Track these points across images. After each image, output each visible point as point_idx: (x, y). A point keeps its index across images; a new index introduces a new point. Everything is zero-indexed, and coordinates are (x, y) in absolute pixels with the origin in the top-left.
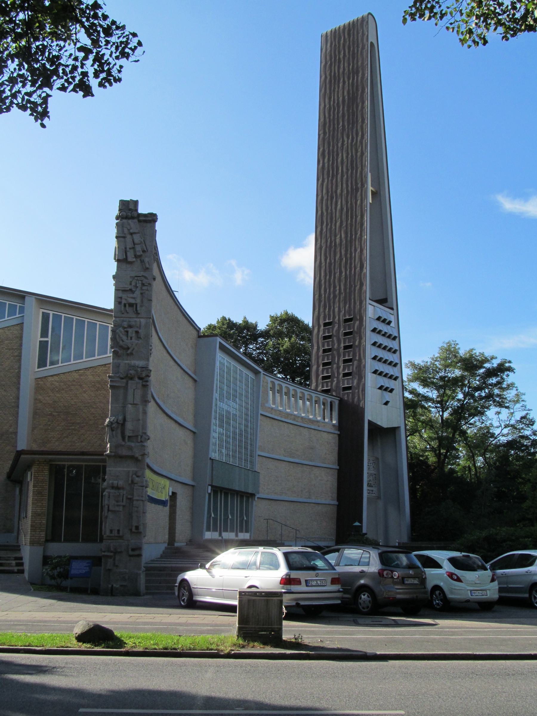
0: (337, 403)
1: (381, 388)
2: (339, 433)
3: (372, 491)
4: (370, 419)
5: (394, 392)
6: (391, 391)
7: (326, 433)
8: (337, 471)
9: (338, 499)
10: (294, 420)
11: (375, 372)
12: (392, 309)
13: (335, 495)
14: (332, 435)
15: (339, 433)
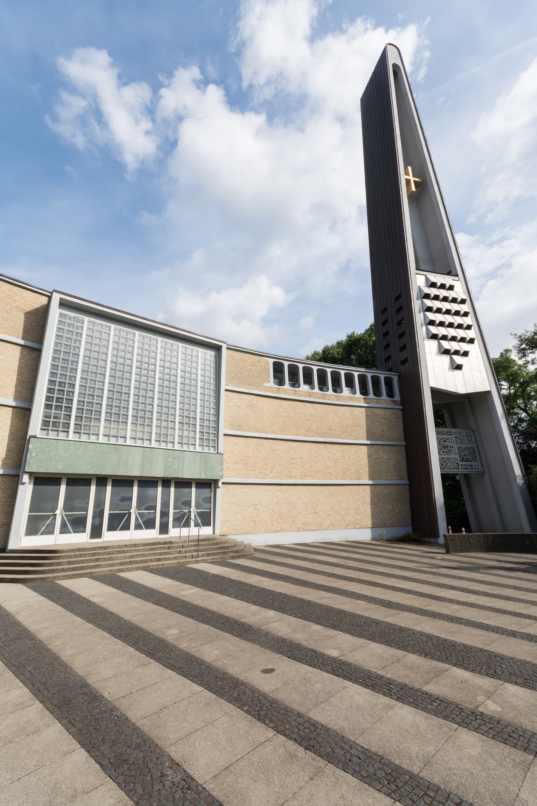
0: (395, 379)
1: (446, 352)
2: (401, 407)
3: (471, 466)
4: (434, 385)
5: (470, 354)
6: (466, 354)
7: (380, 410)
8: (404, 448)
9: (410, 478)
10: (324, 398)
11: (434, 337)
12: (457, 276)
13: (405, 474)
14: (392, 411)
15: (401, 407)
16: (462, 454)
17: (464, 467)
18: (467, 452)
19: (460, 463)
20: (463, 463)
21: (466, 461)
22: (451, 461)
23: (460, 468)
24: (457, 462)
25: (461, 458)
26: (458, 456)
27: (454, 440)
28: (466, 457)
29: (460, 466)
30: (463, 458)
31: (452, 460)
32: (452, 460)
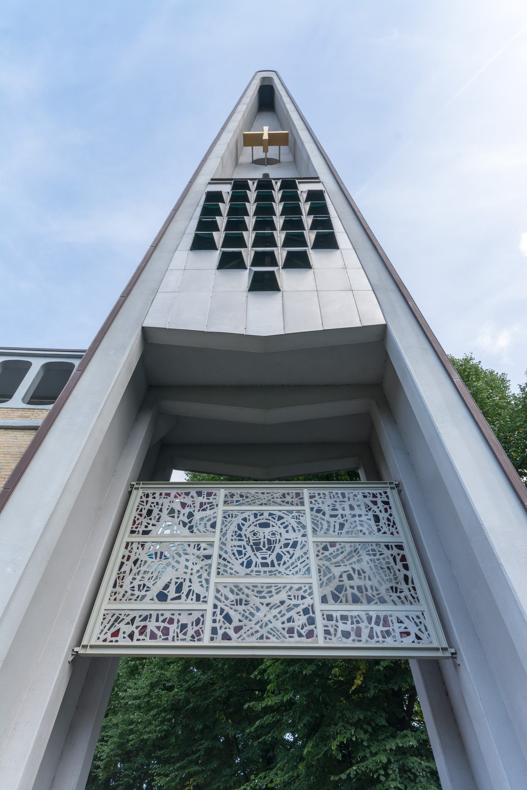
16: (336, 571)
17: (342, 627)
18: (365, 562)
19: (319, 607)
20: (337, 609)
21: (356, 600)
22: (276, 599)
23: (320, 631)
24: (308, 602)
25: (332, 587)
26: (314, 579)
27: (307, 520)
28: (357, 582)
29: (320, 622)
30: (340, 588)
31: (283, 596)
32: (283, 596)
